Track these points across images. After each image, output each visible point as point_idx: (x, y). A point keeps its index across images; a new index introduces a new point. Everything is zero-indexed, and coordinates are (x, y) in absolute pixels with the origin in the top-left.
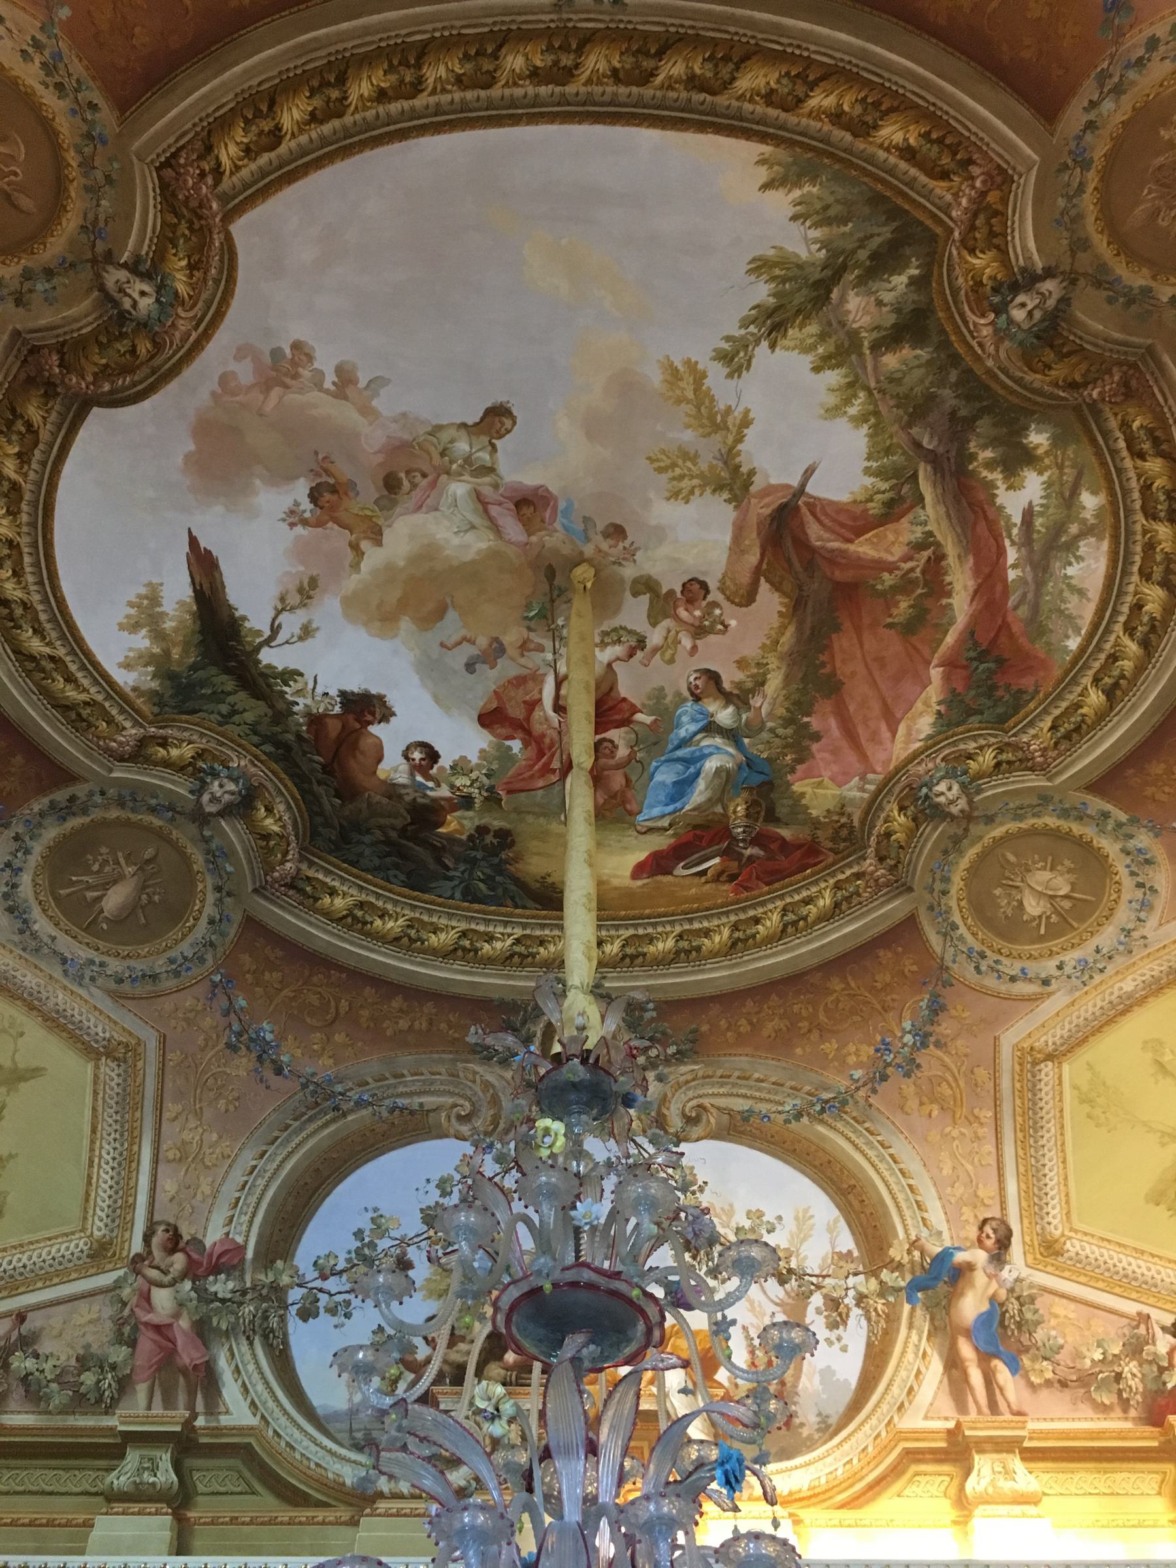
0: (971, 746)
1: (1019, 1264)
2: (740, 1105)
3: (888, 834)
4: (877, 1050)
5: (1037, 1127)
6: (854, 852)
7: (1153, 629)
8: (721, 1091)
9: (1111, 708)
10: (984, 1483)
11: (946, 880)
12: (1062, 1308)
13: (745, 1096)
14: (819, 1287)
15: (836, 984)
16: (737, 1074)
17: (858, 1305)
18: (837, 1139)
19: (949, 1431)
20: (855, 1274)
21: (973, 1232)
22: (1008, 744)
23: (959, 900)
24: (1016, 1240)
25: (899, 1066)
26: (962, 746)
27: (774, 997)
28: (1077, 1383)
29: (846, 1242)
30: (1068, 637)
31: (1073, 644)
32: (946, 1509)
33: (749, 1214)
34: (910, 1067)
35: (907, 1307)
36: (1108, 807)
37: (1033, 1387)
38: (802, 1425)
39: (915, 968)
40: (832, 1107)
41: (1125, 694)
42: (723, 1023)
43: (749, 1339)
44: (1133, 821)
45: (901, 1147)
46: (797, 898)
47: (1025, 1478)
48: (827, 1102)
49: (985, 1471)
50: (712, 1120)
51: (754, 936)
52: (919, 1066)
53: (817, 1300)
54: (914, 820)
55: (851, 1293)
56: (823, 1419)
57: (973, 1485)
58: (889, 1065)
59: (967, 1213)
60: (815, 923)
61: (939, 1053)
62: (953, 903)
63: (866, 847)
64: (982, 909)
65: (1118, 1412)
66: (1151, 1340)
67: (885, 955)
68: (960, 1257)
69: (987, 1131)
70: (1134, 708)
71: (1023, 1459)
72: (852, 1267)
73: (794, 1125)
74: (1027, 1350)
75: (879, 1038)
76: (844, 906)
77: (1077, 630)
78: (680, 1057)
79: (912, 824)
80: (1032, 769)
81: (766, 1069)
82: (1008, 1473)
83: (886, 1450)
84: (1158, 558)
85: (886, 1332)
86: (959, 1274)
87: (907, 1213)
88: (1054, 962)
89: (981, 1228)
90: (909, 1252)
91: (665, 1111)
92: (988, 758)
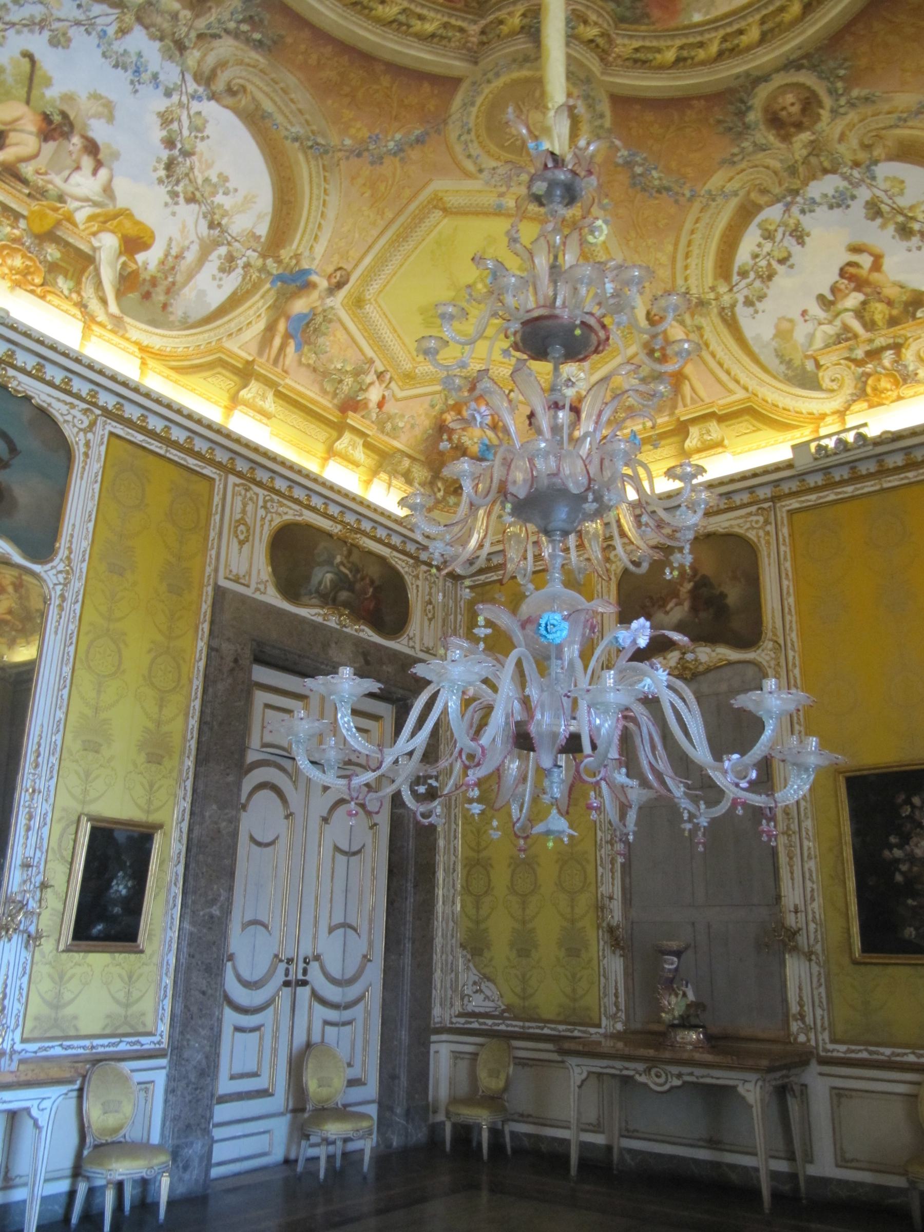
0: (593, 17)
1: (337, 301)
2: (268, 106)
3: (501, 22)
4: (370, 137)
5: (405, 239)
6: (475, 14)
7: (732, 50)
8: (265, 88)
9: (670, 68)
10: (250, 395)
11: (497, 75)
12: (341, 335)
13: (275, 103)
14: (229, 244)
15: (385, 81)
16: (282, 85)
17: (243, 268)
18: (305, 170)
19: (248, 363)
20: (254, 251)
21: (330, 269)
22: (609, 36)
23: (491, 92)
24: (346, 288)
25: (373, 155)
26: (589, 13)
27: (346, 57)
28: (321, 373)
29: (263, 230)
30: (699, 11)
31: (697, 18)
32: (225, 400)
33: (220, 175)
34: (378, 160)
35: (268, 286)
36: (608, 114)
37: (300, 363)
38: (172, 313)
39: (432, 109)
40: (316, 149)
41: (684, 67)
42: (303, 47)
43: (169, 246)
44: (610, 131)
45: (334, 200)
46: (418, 10)
47: (270, 403)
48: (318, 144)
49: (252, 391)
50: (243, 102)
51: (371, 9)
52: (381, 163)
53: (223, 250)
54: (522, 28)
55: (244, 259)
56: (186, 317)
57: (244, 393)
58: (367, 150)
59: (336, 258)
60: (410, 35)
61: (398, 165)
62: (486, 91)
63: (482, 17)
64: (495, 107)
65: (329, 398)
66: (366, 373)
67: (426, 87)
68: (314, 278)
69: (381, 224)
70: (679, 78)
71: (275, 395)
72: (255, 245)
73: (288, 143)
74: (309, 344)
75: (377, 131)
76: (436, 40)
77: (707, 13)
78: (259, 45)
79: (518, 29)
80: (602, 60)
81: (303, 97)
82: (264, 398)
83: (210, 352)
84: (778, 19)
85: (248, 292)
86: (308, 286)
87: (307, 237)
88: (494, 164)
89: (336, 270)
90: (291, 258)
91: (219, 72)
92: (591, 32)
